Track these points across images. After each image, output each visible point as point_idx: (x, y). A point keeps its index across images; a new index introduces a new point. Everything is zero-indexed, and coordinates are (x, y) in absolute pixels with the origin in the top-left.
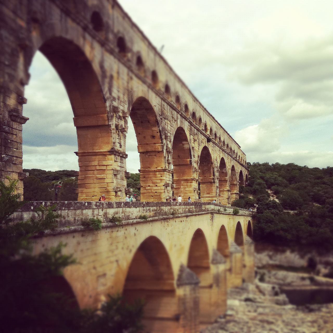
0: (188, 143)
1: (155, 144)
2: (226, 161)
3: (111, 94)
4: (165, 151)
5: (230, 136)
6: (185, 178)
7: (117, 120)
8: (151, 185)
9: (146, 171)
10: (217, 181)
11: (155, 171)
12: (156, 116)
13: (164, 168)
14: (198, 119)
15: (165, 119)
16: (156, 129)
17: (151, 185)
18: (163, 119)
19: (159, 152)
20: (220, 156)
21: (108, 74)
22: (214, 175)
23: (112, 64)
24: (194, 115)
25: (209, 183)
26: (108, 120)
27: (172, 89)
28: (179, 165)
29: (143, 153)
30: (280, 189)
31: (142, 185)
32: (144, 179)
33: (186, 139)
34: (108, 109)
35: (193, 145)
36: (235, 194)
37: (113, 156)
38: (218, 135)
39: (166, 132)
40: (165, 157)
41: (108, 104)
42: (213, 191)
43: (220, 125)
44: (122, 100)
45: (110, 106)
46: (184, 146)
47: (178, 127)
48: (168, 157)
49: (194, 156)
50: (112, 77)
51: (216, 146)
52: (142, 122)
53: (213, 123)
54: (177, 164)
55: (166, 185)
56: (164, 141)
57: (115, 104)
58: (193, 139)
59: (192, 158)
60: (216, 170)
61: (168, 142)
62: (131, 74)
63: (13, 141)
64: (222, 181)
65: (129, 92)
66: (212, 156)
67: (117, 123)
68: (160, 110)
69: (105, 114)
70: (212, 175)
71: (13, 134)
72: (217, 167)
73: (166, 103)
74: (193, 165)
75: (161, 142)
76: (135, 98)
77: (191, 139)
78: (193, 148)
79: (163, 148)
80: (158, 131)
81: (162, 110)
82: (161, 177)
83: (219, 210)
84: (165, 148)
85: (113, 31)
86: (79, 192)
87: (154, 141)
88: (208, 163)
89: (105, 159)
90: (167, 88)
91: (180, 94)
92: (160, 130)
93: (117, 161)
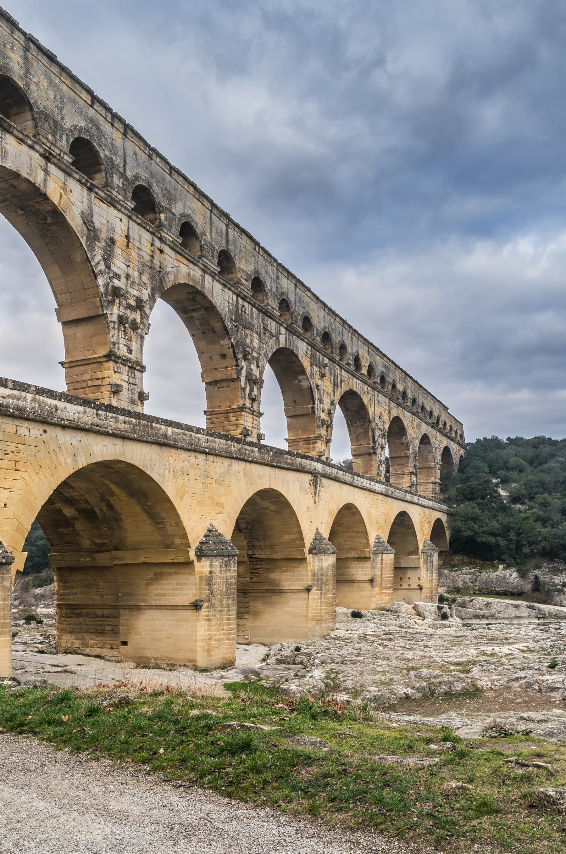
1: (227, 367)
3: (108, 267)
4: (243, 379)
5: (421, 386)
7: (122, 309)
12: (223, 322)
14: (338, 346)
15: (245, 327)
16: (225, 342)
18: (240, 327)
19: (233, 380)
20: (390, 413)
21: (103, 235)
22: (374, 442)
23: (113, 220)
25: (367, 456)
28: (296, 416)
30: (510, 474)
33: (303, 372)
35: (319, 382)
36: (433, 483)
40: (244, 389)
41: (101, 281)
42: (373, 468)
43: (393, 363)
45: (106, 285)
46: (302, 384)
47: (281, 346)
49: (321, 401)
51: (380, 395)
52: (204, 333)
53: (378, 358)
58: (318, 373)
59: (316, 403)
60: (377, 433)
61: (253, 367)
62: (157, 243)
64: (401, 457)
66: (371, 410)
67: (121, 314)
70: (371, 441)
72: (380, 430)
73: (249, 303)
74: (317, 415)
75: (235, 363)
77: (315, 372)
78: (317, 386)
79: (239, 372)
80: (230, 346)
81: (237, 312)
82: (237, 420)
84: (244, 373)
87: (225, 363)
88: (363, 422)
92: (232, 343)
93: (119, 371)
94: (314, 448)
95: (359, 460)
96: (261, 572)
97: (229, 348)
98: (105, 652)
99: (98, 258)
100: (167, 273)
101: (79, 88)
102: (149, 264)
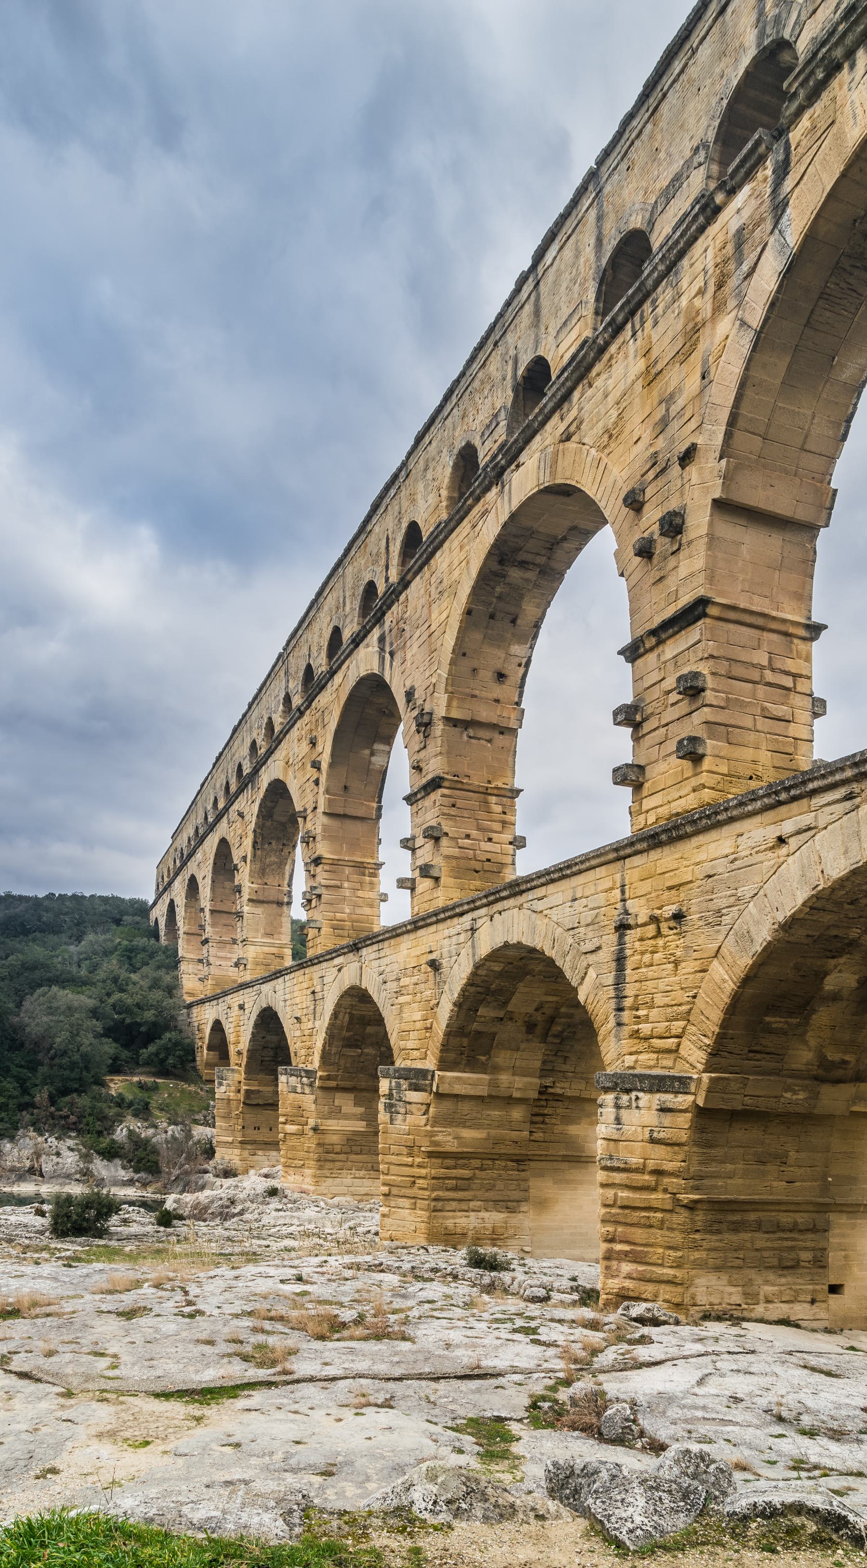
0: (389, 752)
8: (474, 833)
9: (459, 786)
17: (474, 833)
25: (275, 906)
29: (455, 726)
32: (453, 811)
42: (284, 930)
46: (373, 759)
54: (340, 811)
70: (286, 882)
86: (709, 751)
95: (259, 910)
96: (554, 1121)
97: (520, 665)
98: (800, 1311)
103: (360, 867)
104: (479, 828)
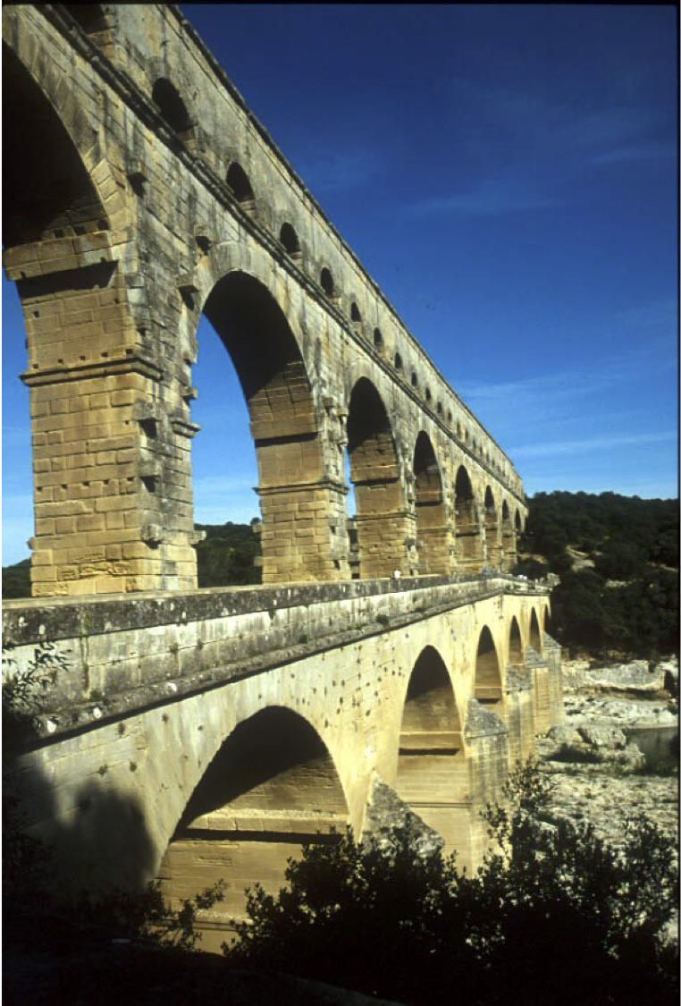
2: (494, 491)
3: (318, 374)
4: (402, 478)
6: (433, 528)
10: (483, 531)
11: (385, 517)
13: (402, 510)
21: (313, 338)
22: (477, 520)
24: (439, 407)
26: (316, 422)
27: (405, 362)
31: (361, 544)
32: (365, 533)
34: (315, 403)
37: (326, 492)
38: (478, 444)
39: (403, 441)
40: (403, 489)
41: (315, 392)
44: (336, 385)
45: (318, 397)
48: (408, 489)
50: (318, 343)
55: (409, 543)
56: (401, 459)
57: (325, 392)
60: (480, 509)
61: (407, 460)
62: (345, 335)
63: (177, 471)
65: (344, 368)
67: (330, 428)
68: (392, 401)
69: (310, 411)
71: (176, 458)
72: (481, 505)
75: (394, 460)
76: (353, 383)
79: (399, 473)
83: (508, 587)
84: (403, 471)
85: (313, 258)
89: (313, 497)
90: (398, 359)
91: (418, 369)
94: (443, 542)
99: (312, 365)
100: (353, 368)
101: (283, 167)
102: (341, 362)
103: (435, 532)
104: (382, 539)
